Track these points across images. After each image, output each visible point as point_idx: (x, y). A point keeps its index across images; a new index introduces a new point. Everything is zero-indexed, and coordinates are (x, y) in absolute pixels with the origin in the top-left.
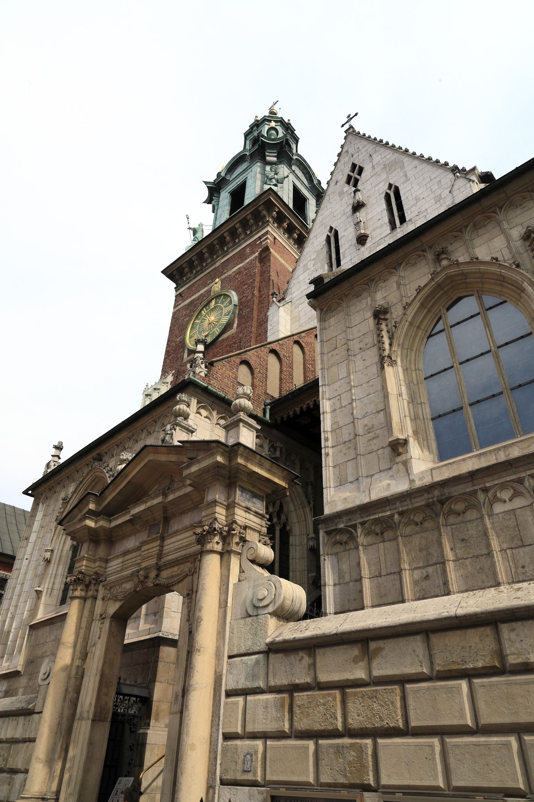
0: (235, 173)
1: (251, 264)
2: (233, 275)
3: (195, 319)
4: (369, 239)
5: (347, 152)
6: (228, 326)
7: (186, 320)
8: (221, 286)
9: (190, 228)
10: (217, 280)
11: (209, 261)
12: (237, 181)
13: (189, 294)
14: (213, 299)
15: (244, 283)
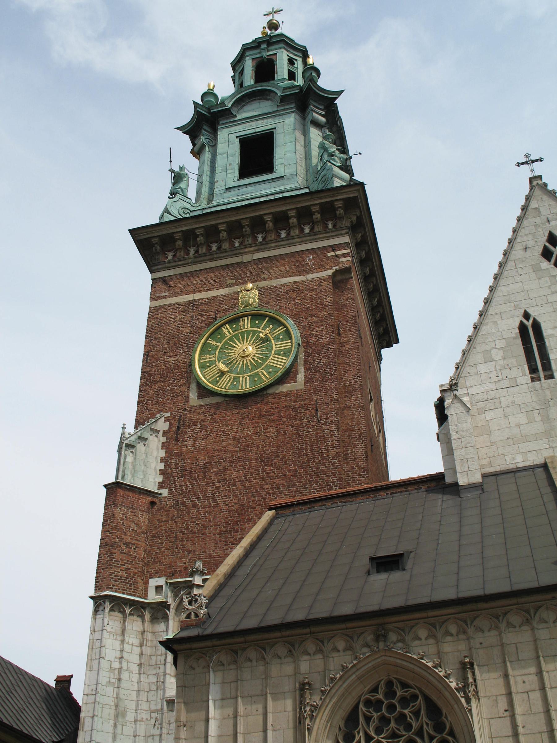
2: (284, 289)
3: (209, 336)
9: (172, 171)
12: (254, 124)
13: (186, 286)
14: (247, 316)
15: (309, 312)
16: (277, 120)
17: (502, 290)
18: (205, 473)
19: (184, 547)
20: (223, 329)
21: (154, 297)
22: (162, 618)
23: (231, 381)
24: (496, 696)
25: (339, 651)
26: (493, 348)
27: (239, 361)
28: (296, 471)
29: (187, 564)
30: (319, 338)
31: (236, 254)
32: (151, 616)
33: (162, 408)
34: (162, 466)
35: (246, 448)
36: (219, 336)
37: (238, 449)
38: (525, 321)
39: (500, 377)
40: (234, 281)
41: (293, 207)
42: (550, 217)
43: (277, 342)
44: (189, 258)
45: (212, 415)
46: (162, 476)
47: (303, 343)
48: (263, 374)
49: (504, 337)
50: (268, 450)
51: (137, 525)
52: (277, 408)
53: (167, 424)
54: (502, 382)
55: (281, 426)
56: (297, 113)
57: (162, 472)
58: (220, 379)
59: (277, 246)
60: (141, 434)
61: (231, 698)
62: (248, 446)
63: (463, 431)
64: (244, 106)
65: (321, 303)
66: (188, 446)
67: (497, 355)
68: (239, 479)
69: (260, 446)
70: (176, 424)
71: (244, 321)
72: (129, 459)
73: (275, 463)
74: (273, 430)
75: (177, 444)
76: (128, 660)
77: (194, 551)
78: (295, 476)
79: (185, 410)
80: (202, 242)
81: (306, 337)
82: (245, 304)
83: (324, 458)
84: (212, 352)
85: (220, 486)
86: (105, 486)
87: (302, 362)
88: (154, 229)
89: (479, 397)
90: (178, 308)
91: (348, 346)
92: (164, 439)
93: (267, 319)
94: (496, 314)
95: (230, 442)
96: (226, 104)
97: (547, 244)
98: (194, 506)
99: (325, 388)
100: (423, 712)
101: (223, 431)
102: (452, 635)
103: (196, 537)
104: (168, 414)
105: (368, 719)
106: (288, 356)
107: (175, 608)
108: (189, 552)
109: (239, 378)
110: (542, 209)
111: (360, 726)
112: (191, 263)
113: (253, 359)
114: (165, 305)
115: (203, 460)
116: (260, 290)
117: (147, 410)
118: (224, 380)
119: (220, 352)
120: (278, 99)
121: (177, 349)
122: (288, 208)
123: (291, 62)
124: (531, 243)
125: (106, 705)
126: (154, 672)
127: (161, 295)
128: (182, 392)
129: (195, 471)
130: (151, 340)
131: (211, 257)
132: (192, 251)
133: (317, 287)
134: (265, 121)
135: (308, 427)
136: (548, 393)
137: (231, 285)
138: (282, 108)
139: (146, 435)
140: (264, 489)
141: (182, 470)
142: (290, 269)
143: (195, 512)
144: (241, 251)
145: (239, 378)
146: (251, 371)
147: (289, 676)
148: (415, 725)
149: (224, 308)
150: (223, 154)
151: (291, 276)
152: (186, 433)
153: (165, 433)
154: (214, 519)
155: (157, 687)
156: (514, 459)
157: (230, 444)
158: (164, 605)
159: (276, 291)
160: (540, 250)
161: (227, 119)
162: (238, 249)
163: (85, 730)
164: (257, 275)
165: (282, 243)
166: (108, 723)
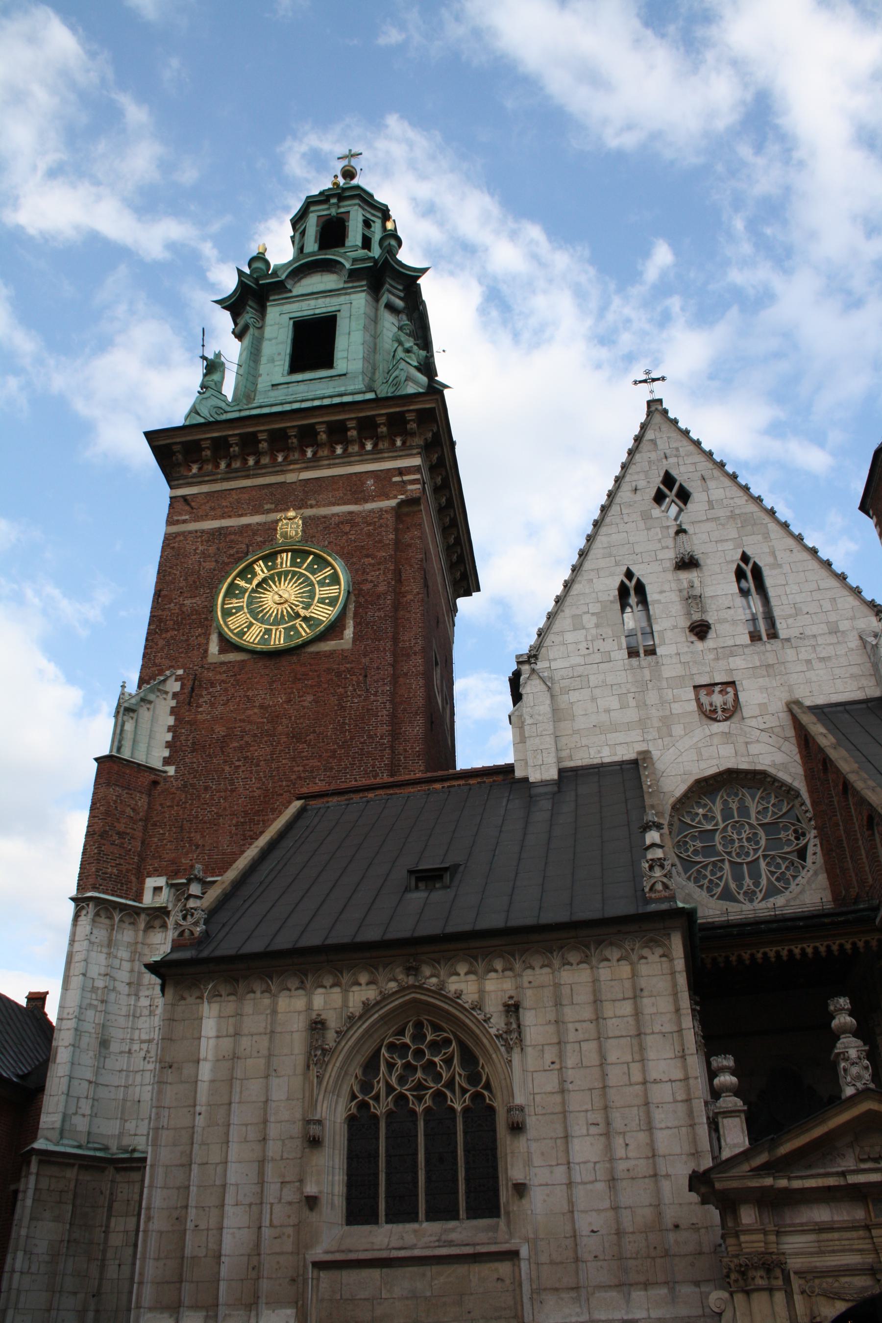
1: (380, 517)
3: (238, 575)
4: (711, 634)
5: (653, 442)
6: (334, 629)
7: (210, 565)
8: (303, 531)
9: (204, 358)
10: (291, 514)
11: (265, 460)
12: (312, 303)
13: (213, 509)
14: (287, 551)
15: (365, 552)
16: (342, 299)
17: (601, 540)
18: (222, 748)
19: (190, 841)
20: (255, 566)
21: (171, 520)
24: (543, 1045)
25: (360, 985)
26: (585, 613)
28: (335, 751)
30: (375, 586)
31: (278, 471)
33: (173, 664)
34: (169, 737)
36: (249, 576)
38: (627, 582)
39: (591, 650)
40: (273, 506)
41: (353, 416)
42: (668, 452)
43: (322, 587)
44: (218, 474)
45: (235, 675)
47: (354, 590)
49: (600, 599)
51: (133, 809)
52: (316, 671)
53: (179, 684)
54: (593, 656)
55: (320, 694)
56: (368, 293)
57: (168, 745)
59: (329, 465)
60: (145, 695)
61: (227, 1036)
62: (277, 717)
63: (539, 715)
65: (380, 541)
66: (204, 713)
67: (589, 621)
70: (189, 684)
71: (282, 559)
72: (129, 726)
73: (310, 740)
74: (310, 698)
75: (189, 710)
77: (204, 846)
78: (333, 757)
79: (202, 667)
80: (237, 453)
81: (359, 583)
82: (285, 535)
83: (370, 737)
84: (240, 595)
85: (239, 766)
86: (96, 759)
89: (563, 673)
90: (201, 536)
91: (410, 597)
92: (173, 703)
93: (311, 557)
94: (592, 570)
97: (662, 487)
98: (206, 788)
99: (378, 649)
100: (455, 1061)
101: (248, 696)
102: (496, 971)
104: (180, 672)
105: (391, 1066)
106: (334, 606)
108: (197, 846)
109: (271, 630)
110: (659, 442)
111: (381, 1075)
112: (221, 479)
114: (184, 532)
115: (220, 730)
116: (305, 520)
117: (155, 665)
119: (249, 596)
121: (196, 588)
122: (347, 416)
123: (367, 224)
124: (641, 484)
126: (147, 993)
127: (179, 518)
128: (199, 644)
130: (164, 576)
132: (223, 465)
133: (376, 520)
134: (328, 300)
135: (353, 697)
136: (647, 672)
138: (350, 285)
139: (151, 697)
141: (194, 743)
142: (345, 494)
145: (271, 630)
146: (287, 623)
147: (299, 1012)
148: (445, 1076)
149: (259, 539)
150: (270, 340)
151: (345, 504)
152: (201, 696)
153: (175, 695)
154: (230, 807)
156: (599, 752)
157: (255, 714)
159: (325, 522)
160: (653, 493)
161: (279, 294)
164: (302, 500)
165: (337, 461)
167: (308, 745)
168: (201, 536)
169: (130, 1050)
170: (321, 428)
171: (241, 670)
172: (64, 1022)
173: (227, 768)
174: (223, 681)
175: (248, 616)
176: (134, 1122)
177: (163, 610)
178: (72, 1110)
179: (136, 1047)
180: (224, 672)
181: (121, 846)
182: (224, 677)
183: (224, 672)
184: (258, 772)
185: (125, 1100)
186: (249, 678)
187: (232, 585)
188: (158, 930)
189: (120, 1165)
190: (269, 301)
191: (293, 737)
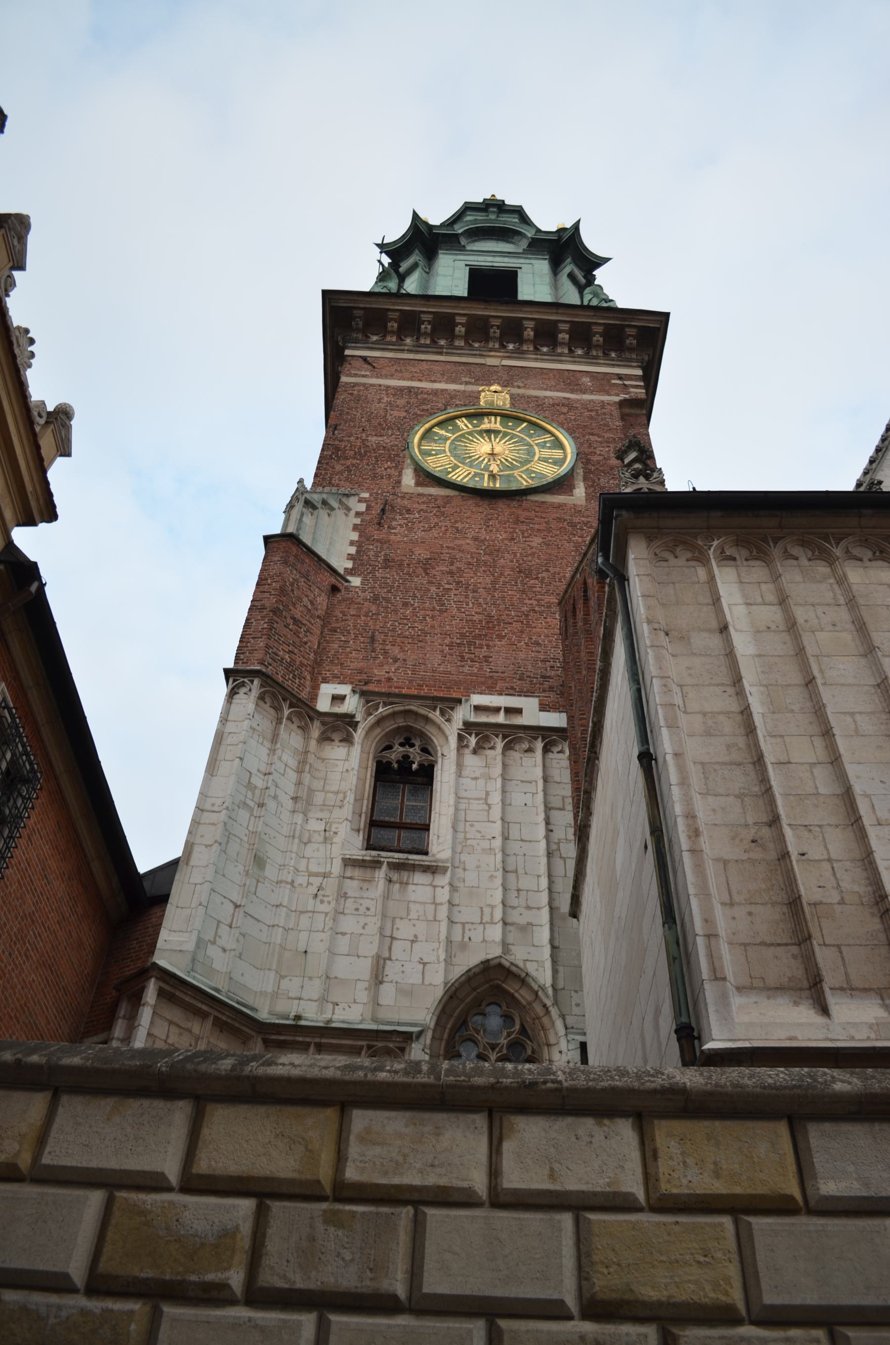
0: (477, 244)
14: (496, 415)
19: (386, 653)
22: (341, 741)
23: (470, 476)
27: (482, 458)
29: (391, 674)
30: (604, 458)
31: (476, 355)
32: (323, 733)
35: (495, 552)
37: (482, 552)
40: (473, 380)
43: (543, 448)
45: (439, 507)
46: (351, 562)
48: (521, 477)
50: (530, 561)
51: (312, 603)
52: (544, 518)
58: (453, 471)
62: (498, 551)
64: (475, 241)
68: (484, 586)
69: (518, 555)
73: (543, 578)
76: (276, 783)
79: (394, 494)
85: (451, 589)
87: (581, 477)
88: (360, 299)
92: (358, 521)
95: (468, 541)
96: (456, 229)
98: (406, 605)
101: (457, 528)
103: (409, 643)
104: (366, 495)
107: (366, 728)
108: (396, 660)
112: (408, 350)
113: (506, 460)
115: (421, 553)
118: (460, 473)
119: (452, 443)
120: (524, 244)
125: (235, 836)
126: (320, 815)
129: (408, 565)
131: (439, 350)
137: (467, 383)
140: (526, 604)
141: (385, 560)
143: (408, 612)
144: (485, 353)
151: (557, 391)
153: (358, 514)
155: (325, 839)
157: (469, 544)
158: (349, 721)
162: (480, 350)
163: (192, 863)
164: (506, 380)
166: (236, 866)
167: (542, 583)
168: (387, 391)
169: (293, 881)
170: (531, 324)
171: (446, 503)
172: (206, 814)
173: (433, 589)
174: (422, 510)
175: (452, 459)
176: (297, 981)
177: (340, 441)
178: (209, 936)
179: (301, 880)
180: (423, 503)
181: (296, 634)
182: (424, 507)
183: (423, 503)
184: (477, 599)
185: (283, 948)
186: (456, 512)
187: (429, 430)
188: (337, 743)
189: (273, 1037)
190: (441, 249)
191: (520, 572)
